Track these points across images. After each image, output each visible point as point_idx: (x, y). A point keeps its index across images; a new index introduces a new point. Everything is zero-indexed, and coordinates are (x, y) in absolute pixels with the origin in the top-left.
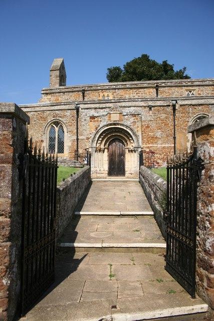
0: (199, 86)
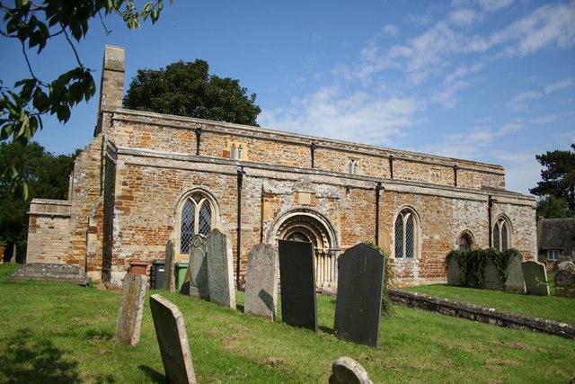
0: (364, 154)
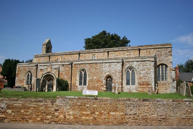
0: (97, 52)
